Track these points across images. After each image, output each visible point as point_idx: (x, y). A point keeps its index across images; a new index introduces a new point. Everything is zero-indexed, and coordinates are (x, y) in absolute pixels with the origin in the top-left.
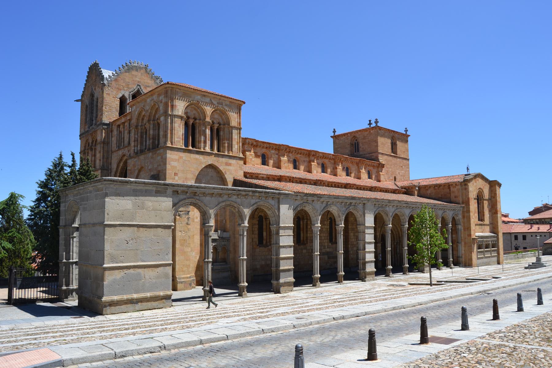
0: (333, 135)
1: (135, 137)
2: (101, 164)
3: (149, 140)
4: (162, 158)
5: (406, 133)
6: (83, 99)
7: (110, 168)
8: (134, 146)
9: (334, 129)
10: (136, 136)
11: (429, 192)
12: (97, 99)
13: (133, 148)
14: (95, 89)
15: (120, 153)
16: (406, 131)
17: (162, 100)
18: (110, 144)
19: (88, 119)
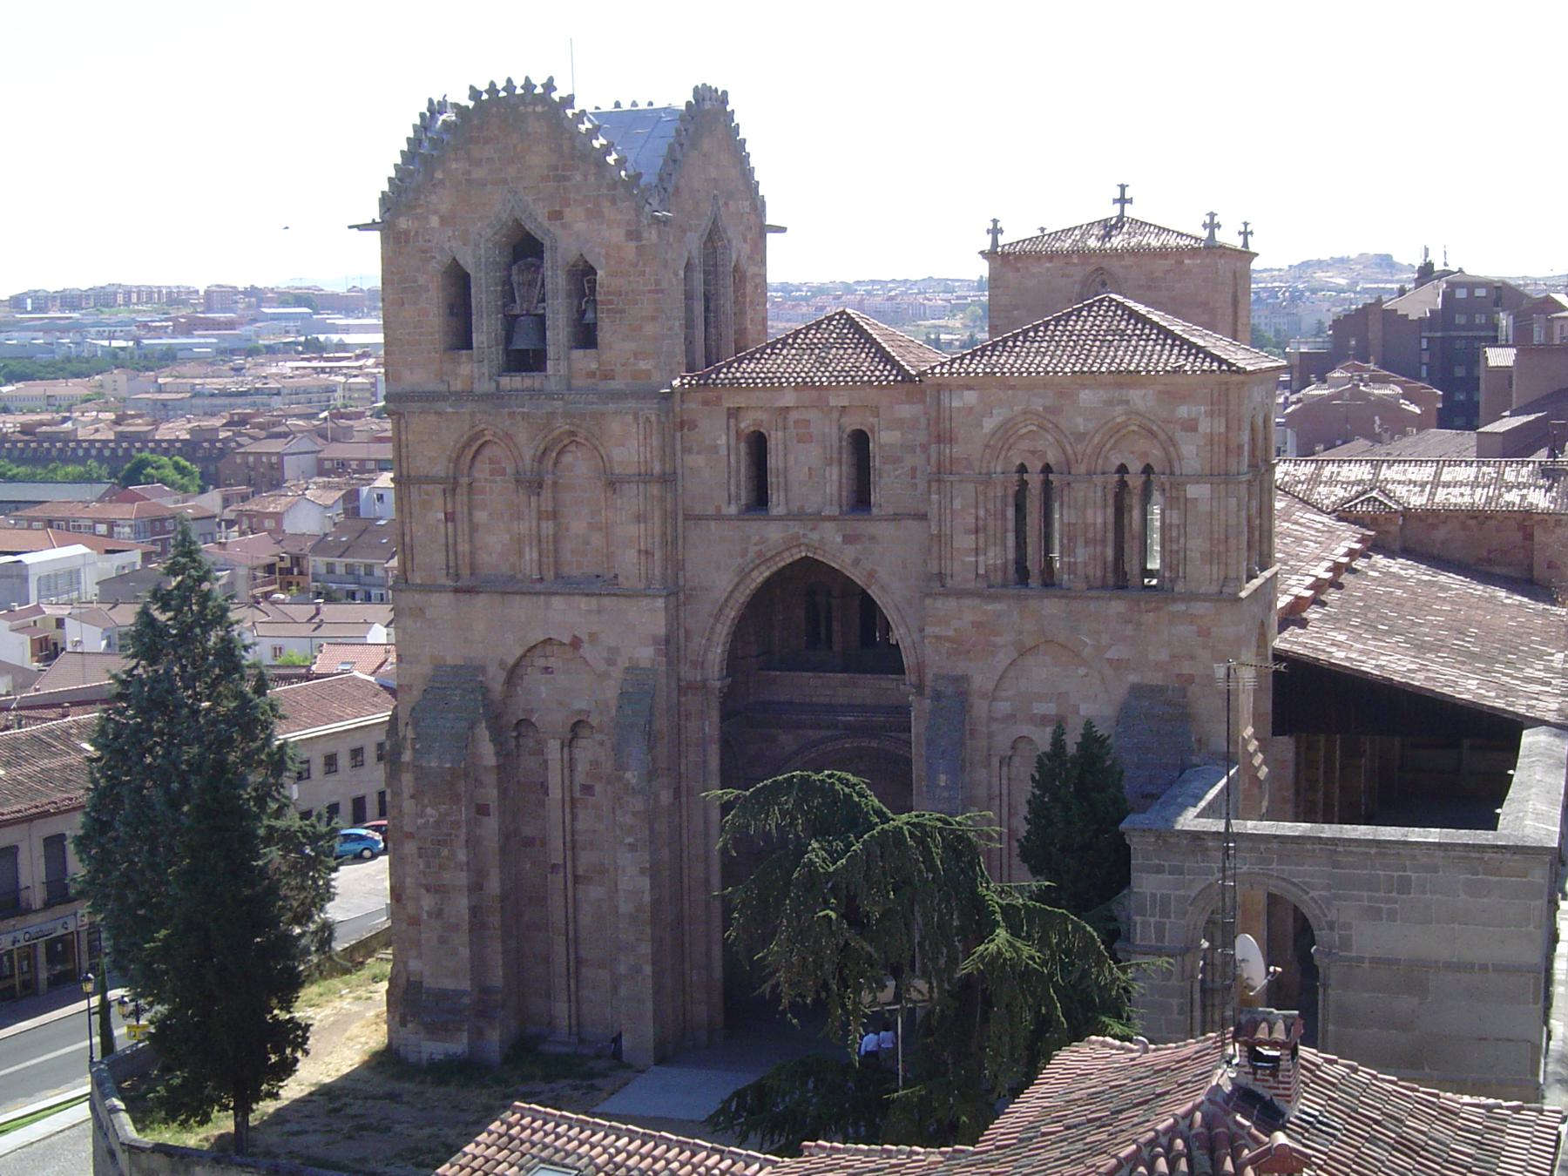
0: (986, 244)
1: (977, 519)
2: (657, 572)
3: (1086, 544)
4: (1204, 633)
5: (1246, 244)
6: (403, 223)
7: (681, 582)
8: (977, 552)
9: (995, 222)
10: (982, 513)
11: (1440, 534)
12: (583, 276)
13: (973, 559)
14: (556, 216)
15: (774, 533)
16: (1246, 234)
17: (1196, 421)
18: (680, 483)
19: (476, 339)
